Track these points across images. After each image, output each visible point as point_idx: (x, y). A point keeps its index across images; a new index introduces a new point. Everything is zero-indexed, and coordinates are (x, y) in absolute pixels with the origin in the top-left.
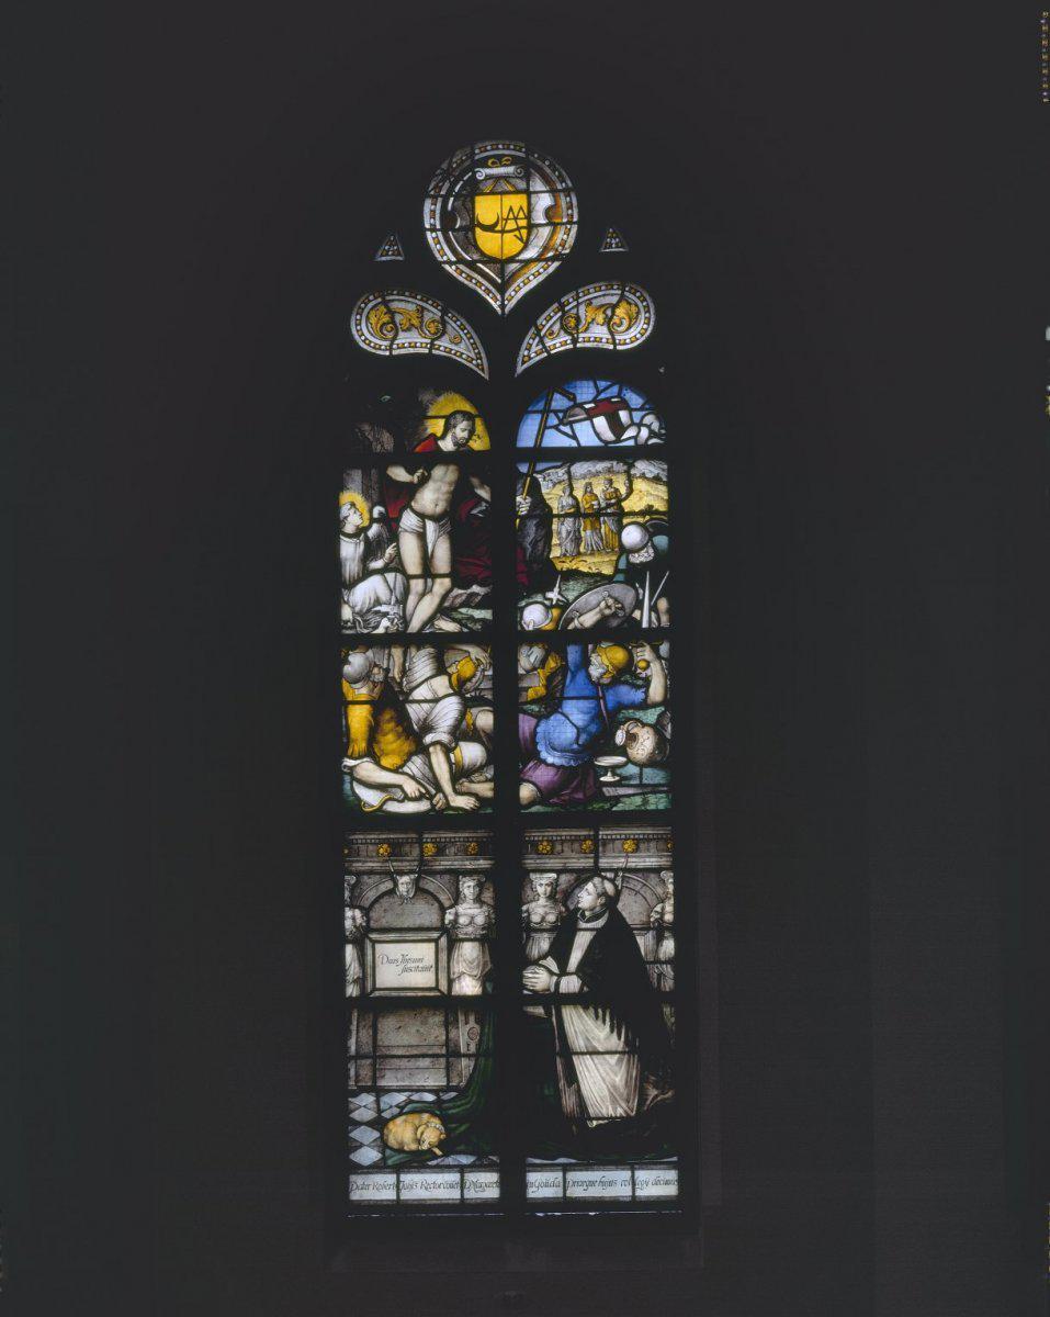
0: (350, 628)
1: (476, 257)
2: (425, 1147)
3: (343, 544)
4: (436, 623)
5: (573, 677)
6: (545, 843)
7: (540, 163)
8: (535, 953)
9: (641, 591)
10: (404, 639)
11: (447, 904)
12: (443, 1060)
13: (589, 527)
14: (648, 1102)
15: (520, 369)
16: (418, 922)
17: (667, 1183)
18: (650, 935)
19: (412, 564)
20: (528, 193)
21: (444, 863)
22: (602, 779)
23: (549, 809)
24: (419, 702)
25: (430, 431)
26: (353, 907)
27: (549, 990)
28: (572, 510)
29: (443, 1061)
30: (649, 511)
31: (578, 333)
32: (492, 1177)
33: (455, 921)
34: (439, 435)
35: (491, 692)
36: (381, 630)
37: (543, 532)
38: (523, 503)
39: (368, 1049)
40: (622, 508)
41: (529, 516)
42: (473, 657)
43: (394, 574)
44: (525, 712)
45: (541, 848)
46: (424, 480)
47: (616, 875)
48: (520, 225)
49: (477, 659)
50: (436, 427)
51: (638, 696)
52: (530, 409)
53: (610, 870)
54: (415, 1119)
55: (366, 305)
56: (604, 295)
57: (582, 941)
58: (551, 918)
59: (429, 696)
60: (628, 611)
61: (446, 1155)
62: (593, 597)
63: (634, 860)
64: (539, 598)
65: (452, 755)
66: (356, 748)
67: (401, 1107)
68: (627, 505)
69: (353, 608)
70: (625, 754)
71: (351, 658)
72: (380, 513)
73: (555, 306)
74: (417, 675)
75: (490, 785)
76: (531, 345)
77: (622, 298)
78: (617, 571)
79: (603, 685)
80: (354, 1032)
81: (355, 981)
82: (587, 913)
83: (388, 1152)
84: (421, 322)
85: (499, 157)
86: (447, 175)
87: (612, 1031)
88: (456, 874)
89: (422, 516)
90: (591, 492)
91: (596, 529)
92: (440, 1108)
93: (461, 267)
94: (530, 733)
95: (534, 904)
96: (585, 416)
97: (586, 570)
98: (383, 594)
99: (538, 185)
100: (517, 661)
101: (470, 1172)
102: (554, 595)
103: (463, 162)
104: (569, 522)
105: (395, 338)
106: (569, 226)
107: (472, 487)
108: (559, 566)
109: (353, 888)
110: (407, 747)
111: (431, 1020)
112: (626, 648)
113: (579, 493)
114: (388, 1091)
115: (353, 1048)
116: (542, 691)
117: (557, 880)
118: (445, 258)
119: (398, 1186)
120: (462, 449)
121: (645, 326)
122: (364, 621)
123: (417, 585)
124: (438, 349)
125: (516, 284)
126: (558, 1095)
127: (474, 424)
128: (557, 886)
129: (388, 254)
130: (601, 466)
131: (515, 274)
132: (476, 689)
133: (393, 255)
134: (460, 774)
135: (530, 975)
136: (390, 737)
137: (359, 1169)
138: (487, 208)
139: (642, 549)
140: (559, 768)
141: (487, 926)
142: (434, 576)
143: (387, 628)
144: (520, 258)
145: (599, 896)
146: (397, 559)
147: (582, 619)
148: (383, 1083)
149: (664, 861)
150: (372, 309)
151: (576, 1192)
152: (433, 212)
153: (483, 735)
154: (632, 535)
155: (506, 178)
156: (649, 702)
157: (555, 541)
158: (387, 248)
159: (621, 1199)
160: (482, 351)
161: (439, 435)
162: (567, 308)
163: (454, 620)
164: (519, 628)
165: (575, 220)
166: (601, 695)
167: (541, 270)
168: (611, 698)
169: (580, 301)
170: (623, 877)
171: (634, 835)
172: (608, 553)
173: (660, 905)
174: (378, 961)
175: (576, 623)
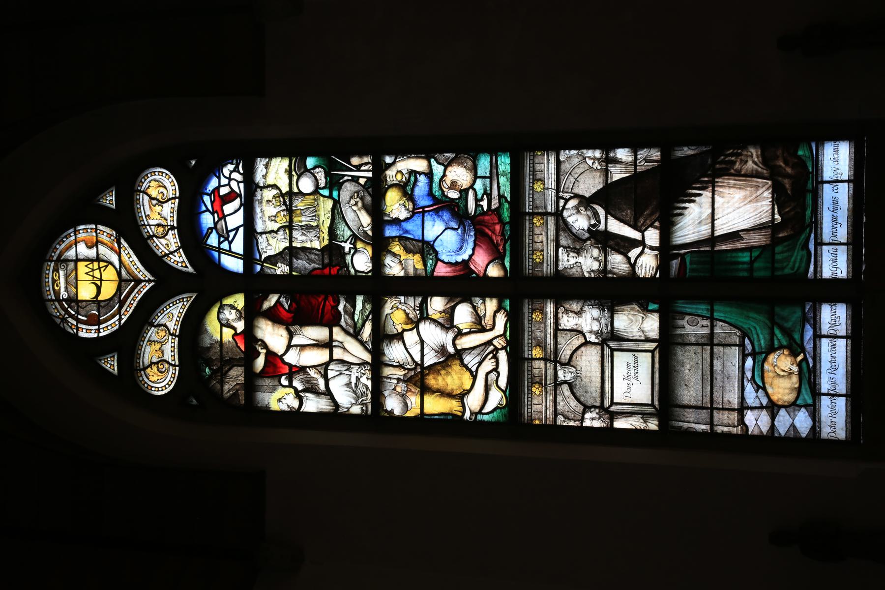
0: (367, 407)
1: (116, 300)
2: (795, 369)
3: (306, 410)
5: (407, 232)
6: (535, 257)
7: (58, 252)
9: (346, 178)
10: (377, 364)
12: (716, 349)
13: (299, 218)
14: (760, 169)
15: (190, 269)
17: (836, 151)
18: (612, 168)
19: (322, 356)
20: (77, 260)
21: (550, 340)
23: (508, 253)
24: (422, 356)
25: (231, 339)
26: (582, 420)
27: (656, 256)
28: (287, 231)
29: (716, 349)
30: (289, 172)
31: (168, 226)
33: (597, 334)
34: (233, 332)
35: (417, 298)
36: (369, 383)
38: (282, 269)
39: (704, 414)
40: (287, 193)
41: (290, 265)
42: (390, 312)
44: (433, 271)
45: (538, 260)
46: (265, 345)
47: (562, 198)
48: (97, 267)
49: (392, 309)
51: (422, 180)
52: (218, 263)
54: (769, 376)
55: (146, 383)
57: (616, 227)
58: (596, 252)
59: (419, 347)
60: (360, 188)
61: (803, 350)
62: (349, 216)
63: (550, 182)
64: (348, 258)
65: (464, 331)
67: (758, 388)
68: (285, 189)
69: (352, 405)
70: (466, 191)
71: (389, 409)
73: (149, 241)
75: (488, 300)
76: (175, 261)
77: (145, 193)
78: (330, 196)
79: (414, 209)
80: (689, 425)
81: (645, 422)
82: (593, 222)
83: (799, 402)
85: (54, 281)
86: (64, 320)
87: (694, 201)
88: (557, 329)
90: (275, 217)
92: (760, 353)
93: (122, 312)
95: (584, 267)
96: (223, 221)
97: (329, 221)
98: (343, 380)
99: (71, 254)
100: (394, 278)
101: (820, 329)
102: (347, 246)
104: (296, 234)
105: (168, 362)
106: (98, 231)
107: (270, 308)
108: (326, 242)
110: (456, 367)
111: (681, 358)
112: (387, 190)
113: (275, 226)
114: (742, 398)
115: (704, 427)
117: (564, 247)
118: (117, 323)
119: (833, 395)
120: (243, 315)
121: (164, 175)
123: (338, 354)
124: (176, 330)
125: (135, 271)
126: (750, 249)
127: (227, 305)
128: (569, 247)
129: (111, 364)
131: (128, 272)
132: (414, 309)
133: (114, 361)
134: (479, 326)
137: (815, 428)
138: (86, 292)
139: (315, 177)
140: (475, 245)
141: (601, 307)
143: (368, 379)
145: (578, 212)
148: (735, 403)
149: (552, 159)
150: (148, 379)
151: (843, 234)
153: (449, 306)
154: (306, 185)
155: (67, 276)
157: (308, 245)
158: (109, 365)
160: (178, 298)
161: (233, 332)
162: (151, 234)
163: (363, 325)
164: (370, 274)
166: (421, 210)
167: (126, 252)
168: (424, 202)
169: (146, 223)
171: (530, 183)
173: (587, 160)
174: (628, 401)
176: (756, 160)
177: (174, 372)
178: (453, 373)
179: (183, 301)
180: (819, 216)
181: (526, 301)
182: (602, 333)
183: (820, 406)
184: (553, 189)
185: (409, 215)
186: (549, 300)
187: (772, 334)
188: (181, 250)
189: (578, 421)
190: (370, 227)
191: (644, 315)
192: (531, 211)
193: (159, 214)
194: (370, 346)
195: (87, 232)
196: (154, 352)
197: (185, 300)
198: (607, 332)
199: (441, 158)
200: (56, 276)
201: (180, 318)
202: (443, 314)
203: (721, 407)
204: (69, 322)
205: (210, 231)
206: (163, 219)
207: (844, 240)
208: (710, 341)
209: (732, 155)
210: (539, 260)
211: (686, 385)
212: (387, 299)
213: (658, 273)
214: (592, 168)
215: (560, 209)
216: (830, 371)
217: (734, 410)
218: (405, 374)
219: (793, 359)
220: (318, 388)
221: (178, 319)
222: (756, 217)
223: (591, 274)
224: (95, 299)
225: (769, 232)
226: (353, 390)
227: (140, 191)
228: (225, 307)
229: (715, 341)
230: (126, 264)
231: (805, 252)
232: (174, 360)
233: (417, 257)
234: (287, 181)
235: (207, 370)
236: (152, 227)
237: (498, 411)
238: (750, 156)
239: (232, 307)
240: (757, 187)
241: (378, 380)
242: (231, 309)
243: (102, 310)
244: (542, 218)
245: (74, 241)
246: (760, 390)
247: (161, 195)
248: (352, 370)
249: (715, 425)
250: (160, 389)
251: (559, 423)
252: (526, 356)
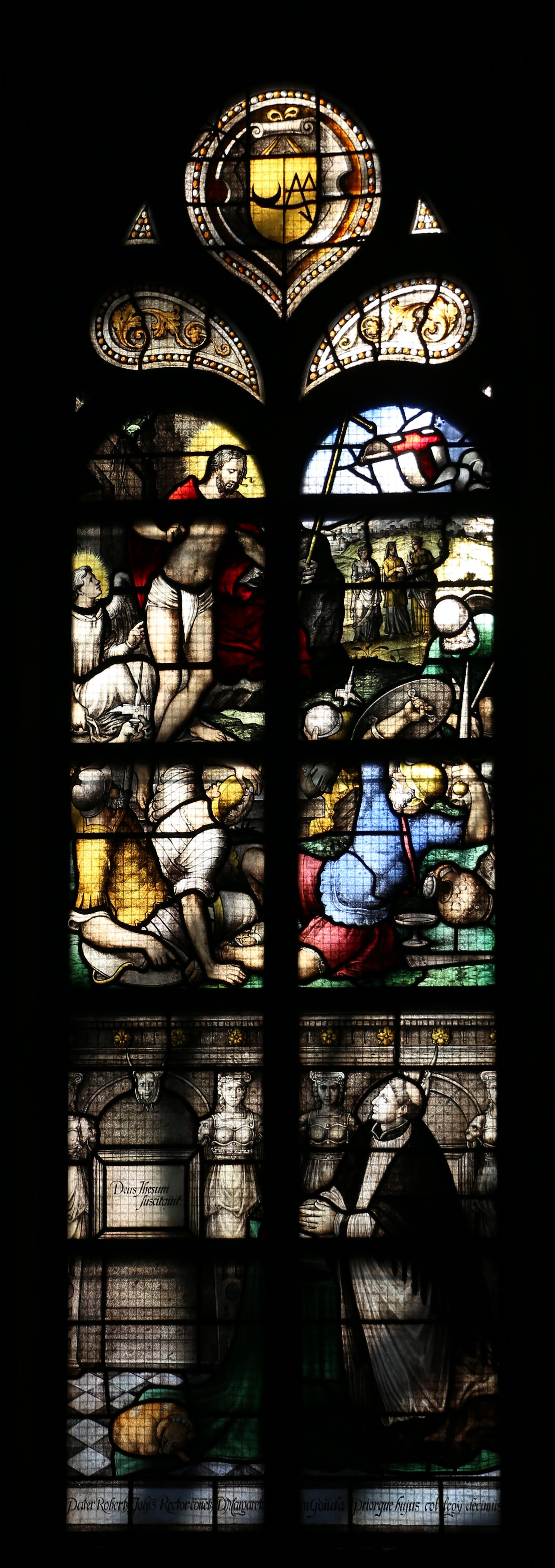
0: (82, 735)
3: (76, 623)
4: (192, 729)
8: (315, 1180)
9: (457, 688)
22: (406, 944)
23: (335, 984)
26: (79, 1115)
28: (369, 579)
30: (469, 581)
31: (380, 342)
33: (212, 1136)
34: (201, 476)
36: (121, 739)
39: (93, 1312)
43: (138, 664)
44: (307, 853)
47: (422, 1076)
56: (414, 292)
59: (183, 829)
64: (327, 698)
66: (87, 897)
69: (85, 708)
70: (436, 910)
72: (123, 581)
75: (258, 951)
79: (407, 816)
81: (79, 1218)
82: (384, 1128)
83: (118, 1456)
84: (180, 328)
89: (178, 586)
98: (126, 691)
102: (344, 693)
105: (145, 348)
106: (369, 200)
107: (241, 548)
110: (153, 896)
112: (438, 766)
114: (120, 1370)
115: (75, 1311)
116: (328, 823)
117: (345, 1081)
122: (101, 726)
123: (169, 679)
124: (201, 363)
127: (245, 463)
133: (145, 237)
135: (309, 1212)
136: (131, 884)
139: (460, 632)
140: (348, 927)
143: (129, 736)
144: (307, 242)
145: (399, 1104)
152: (197, 180)
155: (290, 135)
161: (201, 476)
162: (366, 309)
163: (217, 727)
165: (378, 191)
166: (405, 830)
167: (334, 258)
169: (384, 298)
170: (432, 1079)
176: (476, 1387)
177: (130, 360)
179: (251, 376)
181: (261, 1018)
182: (213, 1146)
184: (436, 1060)
185: (396, 807)
186: (260, 1056)
188: (337, 370)
189: (76, 1108)
190: (377, 736)
192: (402, 1023)
193: (400, 325)
195: (369, 177)
196: (162, 318)
197: (253, 380)
198: (213, 1154)
199: (489, 864)
200: (293, 112)
201: (222, 370)
202: (237, 871)
205: (371, 428)
210: (324, 1038)
212: (260, 770)
213: (307, 1236)
214: (468, 1126)
215: (406, 1074)
216: (165, 1500)
217: (103, 1357)
218: (139, 804)
220: (112, 644)
221: (220, 367)
222: (391, 1388)
223: (303, 1126)
224: (251, 196)
226: (110, 709)
230: (314, 259)
232: (150, 361)
233: (328, 823)
234: (454, 579)
235: (134, 427)
236: (377, 311)
237: (86, 971)
238: (482, 1378)
239: (242, 474)
242: (239, 473)
244: (391, 1042)
245: (352, 149)
246: (132, 1398)
247: (432, 328)
249: (79, 1328)
250: (99, 334)
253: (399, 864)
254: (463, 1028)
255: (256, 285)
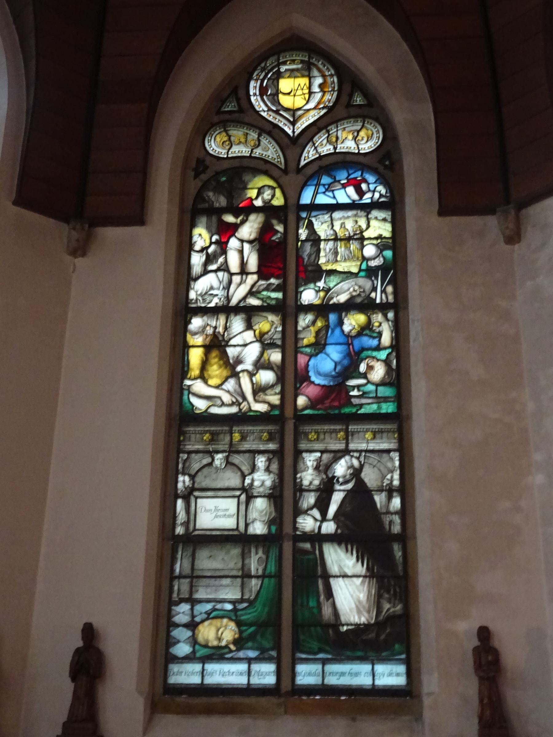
0: (194, 303)
1: (279, 108)
2: (223, 643)
5: (333, 332)
6: (313, 434)
7: (316, 63)
8: (305, 506)
9: (375, 282)
11: (246, 472)
12: (239, 580)
16: (226, 484)
17: (398, 675)
18: (384, 494)
20: (310, 78)
21: (246, 446)
24: (235, 346)
25: (248, 196)
26: (184, 474)
27: (313, 531)
28: (333, 237)
29: (239, 580)
30: (380, 237)
31: (337, 145)
32: (270, 667)
33: (251, 484)
34: (254, 197)
36: (212, 305)
37: (315, 249)
38: (303, 233)
39: (187, 570)
40: (363, 236)
41: (307, 240)
44: (302, 353)
45: (310, 436)
46: (243, 222)
47: (360, 455)
49: (273, 322)
50: (253, 193)
51: (375, 342)
53: (357, 451)
54: (218, 622)
57: (337, 498)
58: (317, 482)
59: (241, 343)
60: (367, 293)
61: (238, 650)
62: (345, 285)
64: (312, 285)
65: (254, 379)
67: (208, 613)
68: (366, 234)
69: (196, 292)
72: (217, 240)
74: (233, 331)
75: (278, 397)
76: (309, 151)
77: (363, 126)
78: (360, 270)
79: (351, 337)
81: (182, 524)
82: (341, 480)
84: (246, 141)
86: (263, 69)
87: (358, 560)
89: (242, 241)
91: (347, 248)
92: (236, 616)
93: (270, 113)
94: (305, 366)
95: (304, 473)
98: (216, 284)
99: (315, 72)
102: (321, 284)
103: (272, 63)
104: (331, 244)
107: (272, 226)
108: (324, 268)
109: (185, 462)
110: (225, 373)
112: (366, 314)
114: (200, 601)
117: (321, 457)
118: (261, 109)
120: (267, 205)
122: (203, 299)
123: (236, 279)
126: (319, 606)
128: (320, 461)
129: (230, 107)
130: (350, 213)
131: (300, 117)
132: (271, 339)
136: (215, 367)
138: (285, 84)
140: (323, 386)
142: (248, 274)
143: (217, 303)
145: (349, 468)
146: (225, 264)
147: (339, 298)
148: (197, 596)
151: (332, 680)
153: (274, 366)
154: (370, 251)
155: (297, 70)
156: (381, 346)
157: (322, 254)
158: (228, 104)
159: (364, 687)
161: (254, 197)
163: (258, 298)
166: (350, 342)
168: (357, 344)
170: (365, 456)
172: (354, 261)
175: (334, 300)
178: (220, 370)
180: (346, 661)
183: (194, 663)
185: (346, 333)
187: (250, 625)
188: (317, 156)
190: (337, 302)
191: (267, 523)
192: (350, 430)
193: (346, 138)
194: (242, 304)
195: (332, 84)
200: (297, 62)
203: (194, 584)
204: (261, 74)
206: (342, 141)
207: (326, 682)
208: (246, 575)
209: (395, 591)
211: (210, 557)
219: (232, 641)
223: (299, 479)
225: (332, 620)
227: (364, 123)
228: (273, 191)
229: (245, 579)
231: (316, 650)
234: (372, 237)
235: (224, 179)
239: (273, 196)
240: (369, 612)
241: (215, 311)
243: (271, 97)
248: (223, 291)
250: (209, 144)
251: (181, 455)
252: (234, 429)
253: (347, 358)
254: (381, 432)
255: (281, 125)
